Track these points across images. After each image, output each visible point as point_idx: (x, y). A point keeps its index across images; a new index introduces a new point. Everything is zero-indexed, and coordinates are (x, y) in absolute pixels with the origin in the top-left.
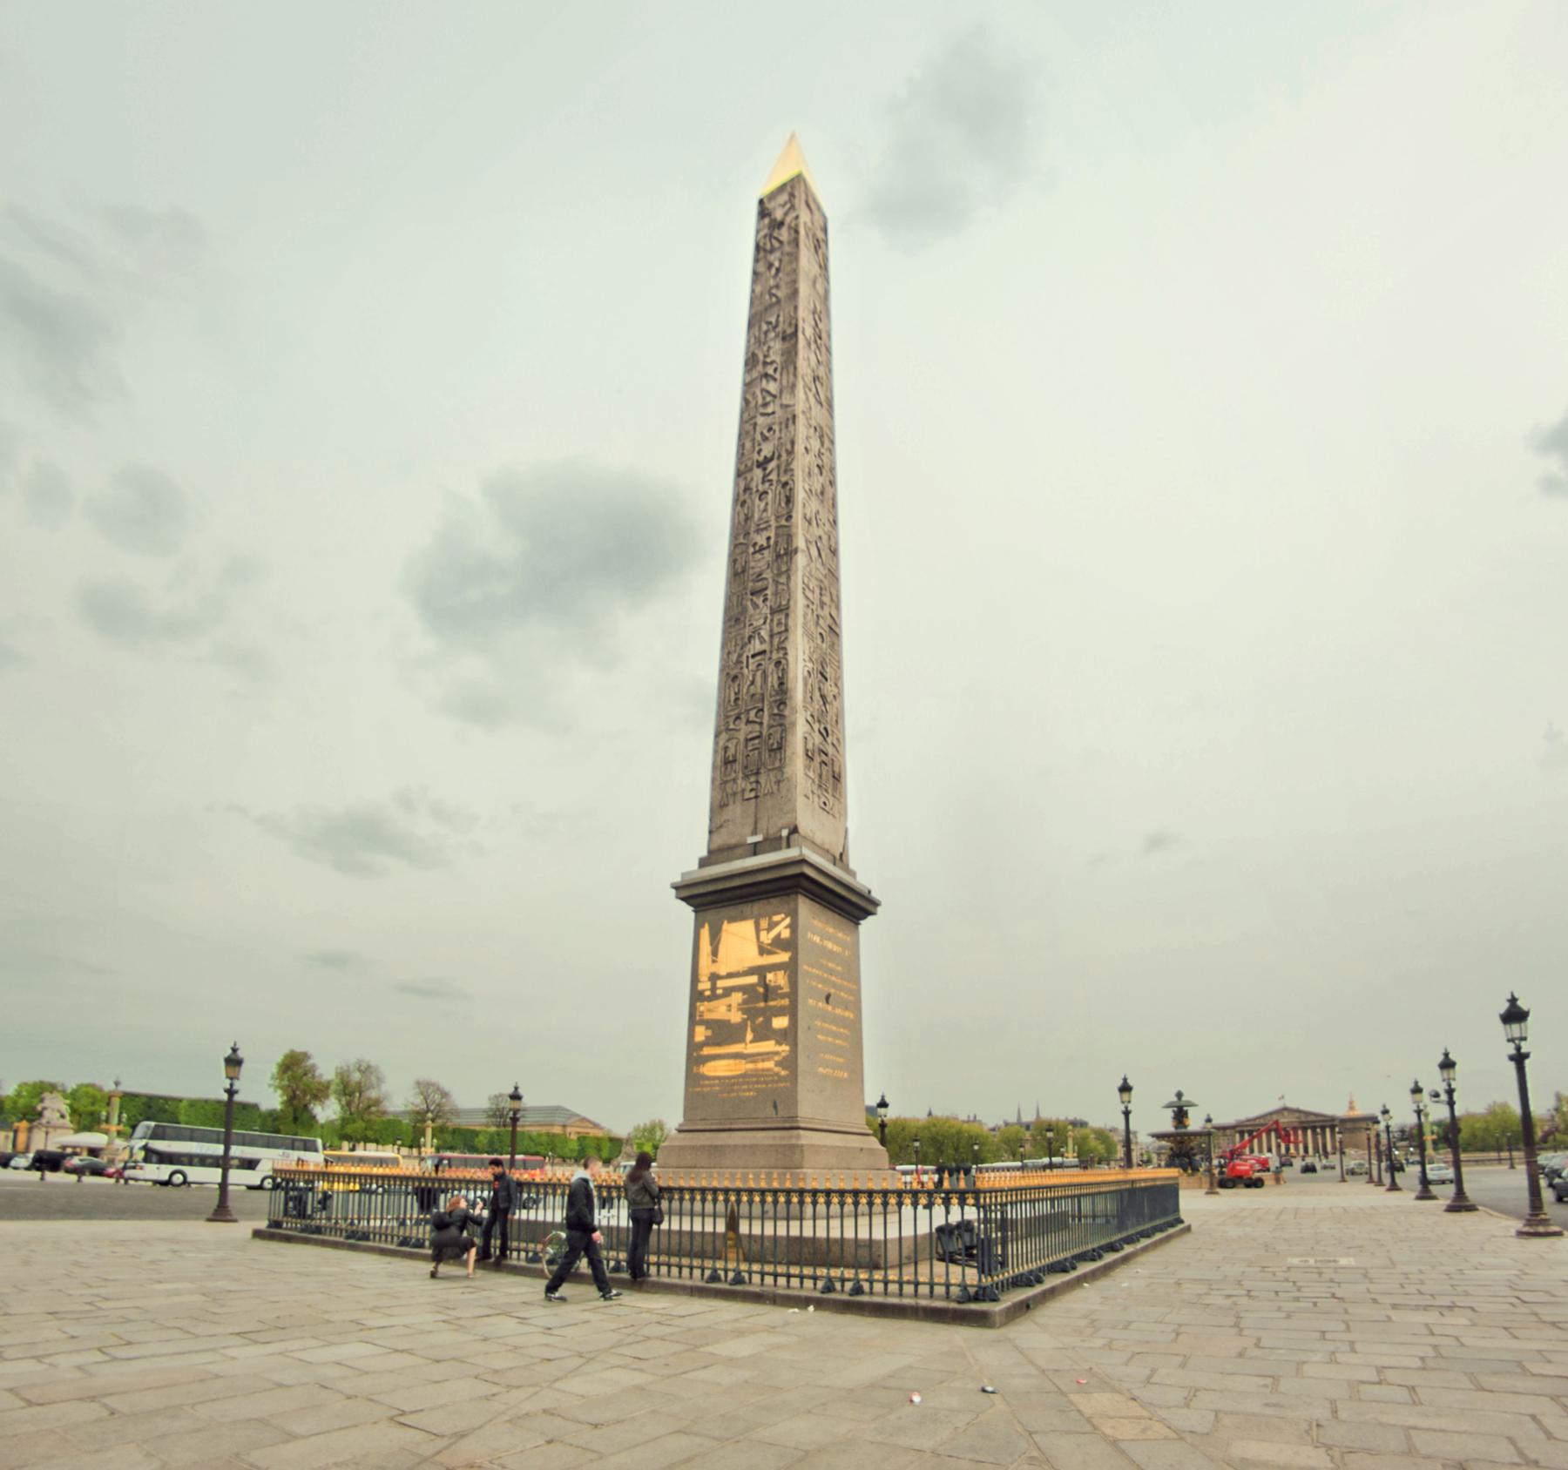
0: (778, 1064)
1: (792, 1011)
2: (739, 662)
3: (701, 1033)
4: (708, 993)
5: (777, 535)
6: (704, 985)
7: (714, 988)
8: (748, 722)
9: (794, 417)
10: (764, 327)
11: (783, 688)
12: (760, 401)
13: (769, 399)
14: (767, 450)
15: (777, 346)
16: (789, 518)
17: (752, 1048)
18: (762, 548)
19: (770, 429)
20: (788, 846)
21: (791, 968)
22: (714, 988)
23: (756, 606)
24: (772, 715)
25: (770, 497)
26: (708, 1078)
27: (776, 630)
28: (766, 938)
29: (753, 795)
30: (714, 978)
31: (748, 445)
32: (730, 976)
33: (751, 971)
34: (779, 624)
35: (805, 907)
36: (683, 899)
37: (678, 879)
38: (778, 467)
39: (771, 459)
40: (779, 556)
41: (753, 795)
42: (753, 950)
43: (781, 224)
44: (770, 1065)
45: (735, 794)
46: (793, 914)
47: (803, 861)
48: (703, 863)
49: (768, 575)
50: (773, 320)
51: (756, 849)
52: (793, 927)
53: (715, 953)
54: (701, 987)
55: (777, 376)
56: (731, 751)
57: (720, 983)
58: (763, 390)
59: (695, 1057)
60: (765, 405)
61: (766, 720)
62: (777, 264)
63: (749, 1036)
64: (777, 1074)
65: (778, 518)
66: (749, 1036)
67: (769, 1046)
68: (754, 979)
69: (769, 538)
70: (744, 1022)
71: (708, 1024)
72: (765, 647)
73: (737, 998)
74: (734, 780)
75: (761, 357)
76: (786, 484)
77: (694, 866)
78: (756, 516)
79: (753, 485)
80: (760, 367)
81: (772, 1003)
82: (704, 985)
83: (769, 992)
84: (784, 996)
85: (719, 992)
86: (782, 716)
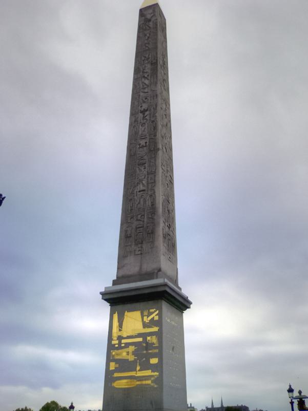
0: (152, 382)
1: (160, 355)
2: (132, 193)
3: (113, 366)
4: (117, 346)
5: (149, 142)
6: (115, 342)
7: (120, 343)
8: (137, 220)
9: (157, 95)
10: (143, 58)
11: (153, 204)
12: (141, 86)
13: (145, 86)
14: (145, 106)
15: (149, 66)
16: (155, 135)
17: (140, 374)
18: (143, 147)
19: (146, 99)
20: (157, 278)
21: (159, 335)
22: (120, 343)
23: (140, 170)
24: (148, 218)
25: (146, 126)
26: (117, 388)
27: (150, 181)
29: (139, 252)
30: (120, 338)
31: (136, 103)
32: (128, 337)
33: (139, 335)
34: (151, 179)
35: (165, 306)
36: (105, 300)
37: (103, 290)
38: (150, 114)
39: (147, 110)
40: (151, 151)
41: (139, 252)
43: (150, 20)
45: (131, 252)
46: (160, 309)
47: (166, 285)
48: (115, 283)
49: (145, 157)
50: (147, 56)
52: (160, 315)
53: (121, 326)
54: (113, 342)
55: (149, 78)
56: (129, 233)
57: (123, 341)
58: (143, 83)
60: (145, 88)
61: (145, 220)
62: (148, 35)
63: (138, 368)
64: (153, 387)
65: (150, 135)
66: (138, 368)
68: (140, 339)
69: (146, 143)
70: (135, 362)
72: (144, 188)
74: (131, 245)
75: (142, 70)
76: (153, 122)
77: (111, 285)
78: (140, 133)
79: (139, 120)
80: (141, 73)
81: (150, 351)
83: (148, 346)
84: (156, 348)
85: (123, 345)
86: (153, 218)
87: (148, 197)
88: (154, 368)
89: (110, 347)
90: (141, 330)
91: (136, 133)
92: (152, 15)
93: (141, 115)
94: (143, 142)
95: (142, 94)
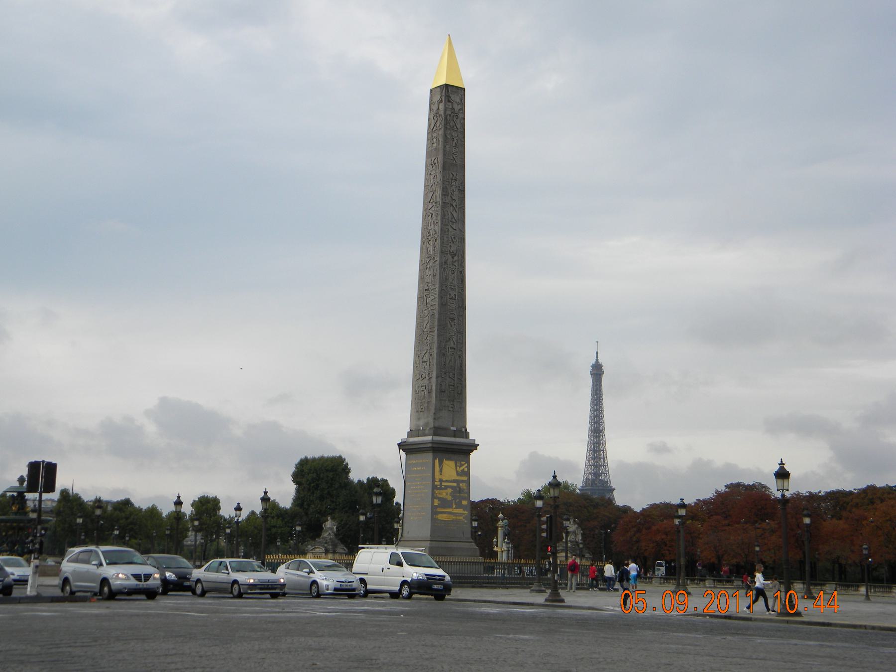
6: (437, 483)
7: (441, 485)
14: (453, 248)
15: (456, 193)
17: (456, 511)
21: (468, 482)
22: (441, 485)
28: (460, 469)
30: (441, 481)
32: (446, 481)
33: (454, 481)
42: (455, 473)
44: (461, 518)
51: (455, 434)
53: (441, 471)
59: (434, 512)
67: (460, 511)
68: (455, 484)
71: (439, 499)
73: (449, 490)
82: (437, 483)
83: (460, 491)
87: (457, 358)
88: (464, 508)
89: (434, 487)
90: (454, 476)
91: (447, 279)
92: (460, 107)
93: (450, 257)
94: (452, 293)
95: (451, 229)
